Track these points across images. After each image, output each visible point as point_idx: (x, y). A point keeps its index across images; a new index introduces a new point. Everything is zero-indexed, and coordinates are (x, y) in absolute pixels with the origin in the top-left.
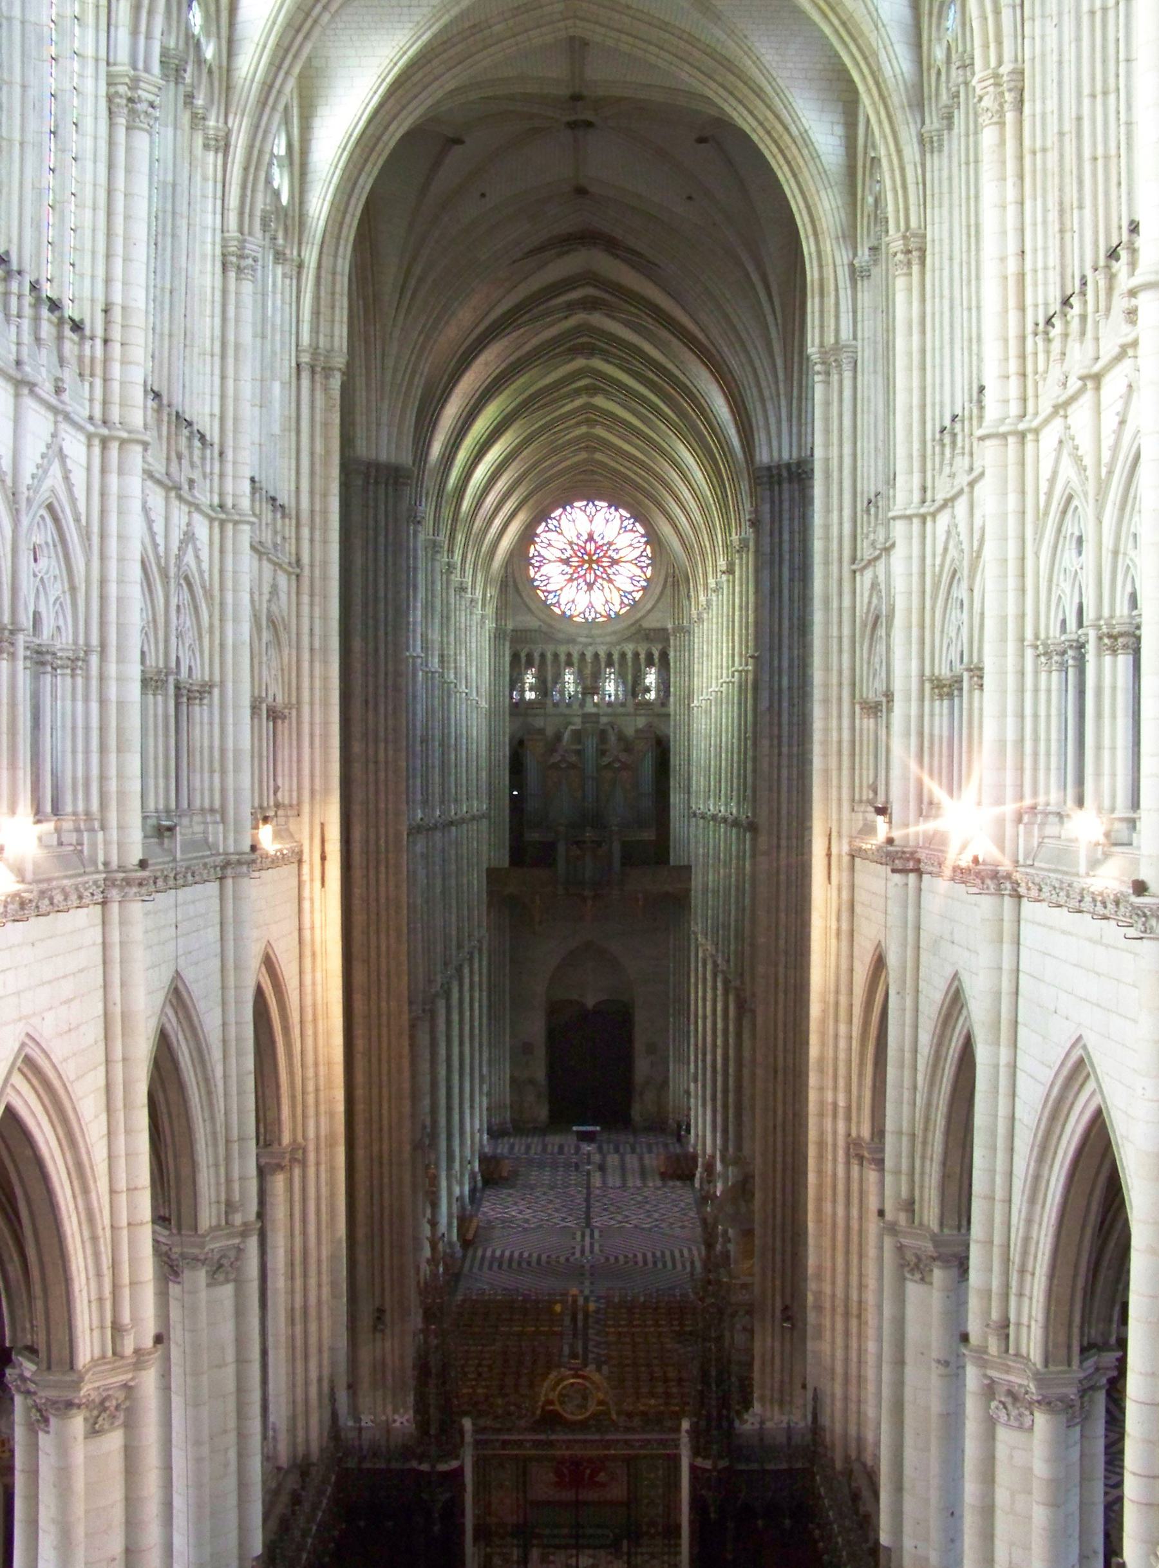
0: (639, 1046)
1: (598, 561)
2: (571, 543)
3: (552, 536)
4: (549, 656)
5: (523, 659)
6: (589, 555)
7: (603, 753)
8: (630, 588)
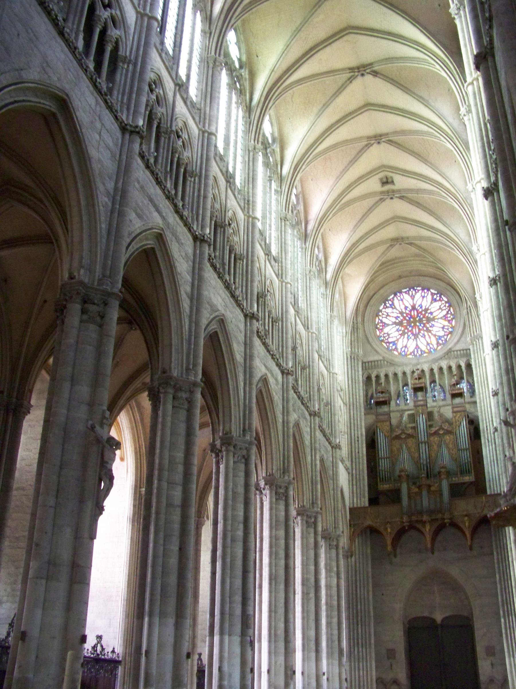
0: (480, 649)
1: (420, 321)
2: (401, 313)
3: (389, 310)
7: (431, 426)
8: (442, 333)
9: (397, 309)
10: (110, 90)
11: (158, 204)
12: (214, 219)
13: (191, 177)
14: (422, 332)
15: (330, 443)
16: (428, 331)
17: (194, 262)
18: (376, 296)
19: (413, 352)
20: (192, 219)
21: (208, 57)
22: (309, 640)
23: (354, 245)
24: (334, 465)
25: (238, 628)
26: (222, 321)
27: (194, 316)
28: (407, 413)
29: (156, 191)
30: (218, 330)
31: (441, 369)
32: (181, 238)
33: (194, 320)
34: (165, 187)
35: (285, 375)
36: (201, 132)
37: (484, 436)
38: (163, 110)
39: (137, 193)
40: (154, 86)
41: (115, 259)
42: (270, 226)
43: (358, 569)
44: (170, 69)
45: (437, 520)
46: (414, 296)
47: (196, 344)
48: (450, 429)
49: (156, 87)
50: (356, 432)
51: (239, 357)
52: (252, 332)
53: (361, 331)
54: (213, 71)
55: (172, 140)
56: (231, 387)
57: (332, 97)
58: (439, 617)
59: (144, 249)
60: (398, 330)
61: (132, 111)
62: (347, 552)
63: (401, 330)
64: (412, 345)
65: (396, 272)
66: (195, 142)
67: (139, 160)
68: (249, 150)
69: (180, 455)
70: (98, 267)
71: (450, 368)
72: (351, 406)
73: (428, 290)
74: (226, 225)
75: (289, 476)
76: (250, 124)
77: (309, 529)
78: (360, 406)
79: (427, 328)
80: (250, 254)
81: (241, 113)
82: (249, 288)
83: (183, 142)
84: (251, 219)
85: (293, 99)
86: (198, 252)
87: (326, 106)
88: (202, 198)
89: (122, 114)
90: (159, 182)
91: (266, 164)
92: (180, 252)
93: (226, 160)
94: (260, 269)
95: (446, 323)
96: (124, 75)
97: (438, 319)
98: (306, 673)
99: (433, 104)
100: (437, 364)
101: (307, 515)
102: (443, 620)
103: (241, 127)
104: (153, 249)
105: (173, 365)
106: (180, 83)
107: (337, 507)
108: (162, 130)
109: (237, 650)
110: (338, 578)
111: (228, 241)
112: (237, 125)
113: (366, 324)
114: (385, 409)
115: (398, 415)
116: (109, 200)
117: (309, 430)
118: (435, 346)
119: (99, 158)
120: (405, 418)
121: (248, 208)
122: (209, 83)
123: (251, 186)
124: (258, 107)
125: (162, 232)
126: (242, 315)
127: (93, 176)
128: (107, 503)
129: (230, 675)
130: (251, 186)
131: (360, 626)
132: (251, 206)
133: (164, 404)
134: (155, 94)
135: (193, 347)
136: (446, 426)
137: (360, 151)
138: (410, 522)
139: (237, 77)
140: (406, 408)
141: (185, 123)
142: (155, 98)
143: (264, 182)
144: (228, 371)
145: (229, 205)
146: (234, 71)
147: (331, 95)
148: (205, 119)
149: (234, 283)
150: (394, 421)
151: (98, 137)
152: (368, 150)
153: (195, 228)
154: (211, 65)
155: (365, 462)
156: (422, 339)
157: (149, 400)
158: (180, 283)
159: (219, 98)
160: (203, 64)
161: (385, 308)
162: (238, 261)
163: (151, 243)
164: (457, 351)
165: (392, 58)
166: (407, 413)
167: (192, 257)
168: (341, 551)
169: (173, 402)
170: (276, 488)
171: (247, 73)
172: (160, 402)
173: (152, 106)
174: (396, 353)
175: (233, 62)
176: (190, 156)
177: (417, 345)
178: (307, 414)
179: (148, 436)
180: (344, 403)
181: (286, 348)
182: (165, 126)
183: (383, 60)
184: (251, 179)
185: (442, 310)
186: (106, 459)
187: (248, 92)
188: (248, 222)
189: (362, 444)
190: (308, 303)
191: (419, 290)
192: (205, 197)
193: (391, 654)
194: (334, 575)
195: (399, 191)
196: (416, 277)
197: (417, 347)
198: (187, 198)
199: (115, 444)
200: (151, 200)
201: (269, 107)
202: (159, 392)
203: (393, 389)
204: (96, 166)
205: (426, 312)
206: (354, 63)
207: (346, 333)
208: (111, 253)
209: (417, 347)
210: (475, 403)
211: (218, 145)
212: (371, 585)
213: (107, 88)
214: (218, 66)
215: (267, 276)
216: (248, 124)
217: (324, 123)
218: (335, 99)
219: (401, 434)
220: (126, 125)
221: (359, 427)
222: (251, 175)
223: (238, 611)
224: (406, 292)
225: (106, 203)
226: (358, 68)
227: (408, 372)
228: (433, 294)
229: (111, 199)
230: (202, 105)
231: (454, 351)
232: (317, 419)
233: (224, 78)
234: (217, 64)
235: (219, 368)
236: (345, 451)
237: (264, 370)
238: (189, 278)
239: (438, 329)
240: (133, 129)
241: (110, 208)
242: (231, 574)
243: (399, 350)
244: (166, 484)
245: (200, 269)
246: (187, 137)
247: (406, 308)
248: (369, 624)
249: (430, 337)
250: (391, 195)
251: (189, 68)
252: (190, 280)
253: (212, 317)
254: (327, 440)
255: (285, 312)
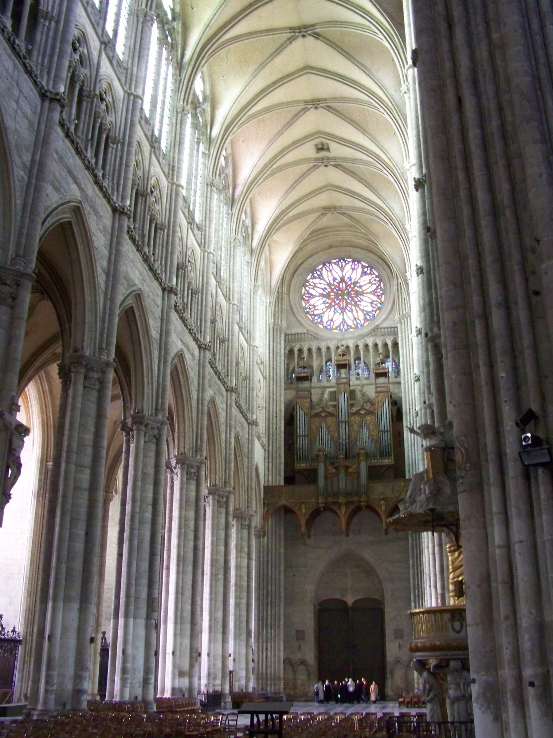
1: (349, 294)
2: (329, 285)
3: (317, 281)
4: (314, 350)
5: (296, 353)
6: (342, 291)
7: (352, 405)
8: (370, 309)
9: (325, 281)
10: (29, 52)
11: (76, 175)
12: (136, 187)
13: (114, 144)
14: (350, 306)
15: (246, 420)
16: (356, 305)
17: (112, 235)
18: (305, 265)
19: (339, 326)
20: (113, 189)
21: (138, 10)
22: (216, 621)
23: (284, 212)
24: (250, 442)
25: (143, 611)
26: (139, 297)
27: (109, 294)
28: (328, 390)
29: (75, 162)
30: (134, 305)
31: (367, 346)
32: (99, 210)
33: (109, 297)
34: (85, 157)
35: (202, 350)
36: (126, 95)
37: (407, 419)
38: (87, 72)
39: (55, 164)
40: (78, 45)
41: (29, 236)
42: (195, 192)
43: (270, 549)
44: (96, 25)
45: (352, 502)
46: (344, 268)
47: (110, 322)
48: (371, 410)
49: (80, 46)
50: (275, 407)
51: (155, 334)
52: (169, 307)
53: (285, 302)
54: (143, 26)
55: (94, 105)
56: (144, 364)
57: (270, 56)
58: (350, 600)
59: (61, 223)
60: (324, 303)
61: (52, 76)
62: (259, 532)
63: (327, 303)
64: (338, 319)
65: (326, 242)
66: (120, 105)
67: (59, 129)
68: (177, 112)
69: (89, 437)
70: (11, 246)
71: (376, 345)
72: (270, 380)
73: (359, 262)
74: (148, 193)
75: (201, 456)
76: (180, 83)
77: (220, 509)
78: (280, 380)
79: (355, 302)
80: (172, 224)
81: (171, 70)
82: (169, 260)
83: (107, 105)
84: (174, 187)
85: (229, 56)
86: (117, 224)
87: (262, 66)
88: (124, 167)
89: (42, 79)
90: (79, 152)
91: (195, 126)
92: (97, 225)
93: (151, 122)
94: (181, 239)
95: (375, 298)
96: (45, 33)
97: (367, 293)
98: (212, 654)
99: (375, 73)
100: (362, 341)
101: (219, 495)
102: (355, 602)
103: (170, 86)
104: (70, 223)
105: (85, 344)
106: (106, 40)
107: (251, 486)
108: (85, 93)
109: (142, 633)
110: (249, 558)
111: (149, 210)
112: (166, 83)
113: (291, 294)
114: (306, 384)
115: (319, 391)
116: (25, 173)
117: (225, 406)
118: (362, 322)
119: (16, 128)
120: (326, 396)
121: (173, 175)
122: (138, 40)
123: (177, 151)
124: (189, 64)
125: (80, 205)
126: (160, 289)
127: (9, 148)
128: (14, 491)
129: (134, 657)
130: (177, 151)
131: (269, 607)
132: (175, 173)
133: (75, 384)
134: (78, 53)
135: (107, 325)
136: (368, 407)
137: (296, 116)
138: (326, 503)
139: (169, 30)
140: (328, 384)
141: (109, 84)
142: (78, 58)
143: (191, 145)
144: (143, 348)
145: (152, 172)
146: (166, 23)
147: (268, 55)
148: (131, 80)
149: (153, 254)
150: (315, 398)
151: (15, 106)
152: (305, 115)
153: (115, 199)
154: (141, 20)
155: (283, 439)
156: (349, 314)
157: (60, 378)
158: (96, 258)
159: (148, 55)
160: (132, 18)
161: (313, 279)
162: (159, 231)
163: (67, 216)
164: (384, 328)
165: (336, 22)
166: (328, 390)
167: (110, 230)
168: (253, 532)
169: (84, 382)
170: (188, 468)
171: (180, 25)
172: (71, 381)
173: (75, 67)
174: (321, 326)
175: (166, 14)
176: (114, 121)
177: (343, 319)
178: (223, 389)
179: (57, 415)
180: (264, 377)
181: (205, 322)
182: (88, 89)
183: (326, 22)
184: (177, 143)
185: (372, 284)
186: (14, 446)
187: (180, 46)
188: (171, 190)
189: (280, 420)
190: (231, 273)
191: (349, 262)
192: (127, 166)
193: (300, 635)
194: (245, 556)
195: (334, 159)
196: (347, 248)
197: (344, 322)
198: (108, 167)
199: (23, 430)
200: (70, 172)
201: (201, 65)
202: (70, 371)
203: (315, 364)
204: (12, 138)
205: (355, 286)
206: (294, 22)
207: (270, 303)
208: (25, 231)
209: (344, 322)
210: (399, 383)
211: (144, 107)
212: (282, 566)
213: (26, 48)
214: (149, 21)
215: (188, 246)
216: (178, 83)
217: (259, 84)
218: (272, 59)
219: (321, 412)
220: (46, 91)
221: (278, 402)
222: (178, 139)
223: (144, 594)
224: (335, 263)
225: (22, 177)
226: (299, 28)
227: (333, 348)
228: (363, 267)
229: (28, 172)
230: (130, 65)
231: (381, 328)
232: (234, 394)
233: (155, 32)
234: (148, 18)
235: (133, 344)
236: (262, 427)
237: (180, 345)
238: (106, 253)
239: (366, 304)
240: (53, 97)
241: (26, 183)
242: (138, 556)
243: (325, 324)
244: (74, 466)
245: (118, 243)
246: (111, 100)
247: (334, 279)
248: (279, 606)
249: (357, 313)
250: (326, 162)
251: (117, 22)
252: (107, 254)
253: (128, 292)
254: (244, 416)
255: (205, 284)
